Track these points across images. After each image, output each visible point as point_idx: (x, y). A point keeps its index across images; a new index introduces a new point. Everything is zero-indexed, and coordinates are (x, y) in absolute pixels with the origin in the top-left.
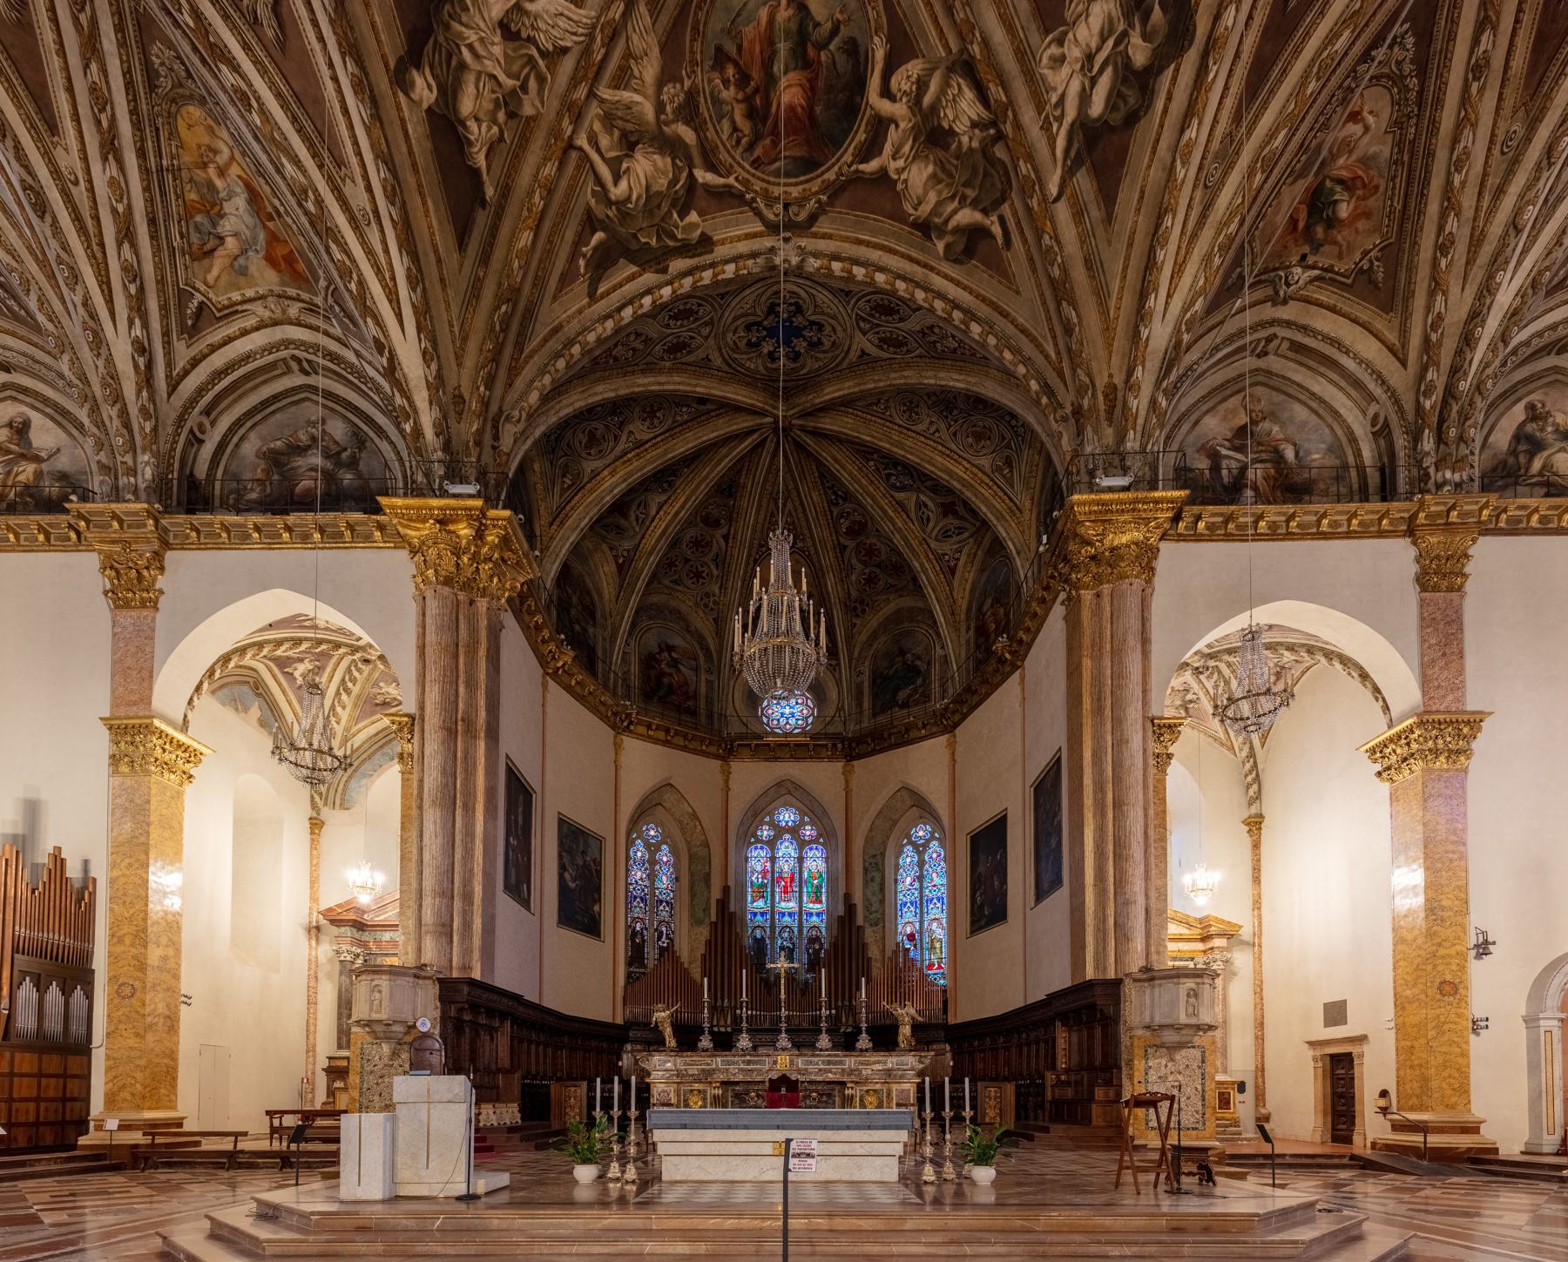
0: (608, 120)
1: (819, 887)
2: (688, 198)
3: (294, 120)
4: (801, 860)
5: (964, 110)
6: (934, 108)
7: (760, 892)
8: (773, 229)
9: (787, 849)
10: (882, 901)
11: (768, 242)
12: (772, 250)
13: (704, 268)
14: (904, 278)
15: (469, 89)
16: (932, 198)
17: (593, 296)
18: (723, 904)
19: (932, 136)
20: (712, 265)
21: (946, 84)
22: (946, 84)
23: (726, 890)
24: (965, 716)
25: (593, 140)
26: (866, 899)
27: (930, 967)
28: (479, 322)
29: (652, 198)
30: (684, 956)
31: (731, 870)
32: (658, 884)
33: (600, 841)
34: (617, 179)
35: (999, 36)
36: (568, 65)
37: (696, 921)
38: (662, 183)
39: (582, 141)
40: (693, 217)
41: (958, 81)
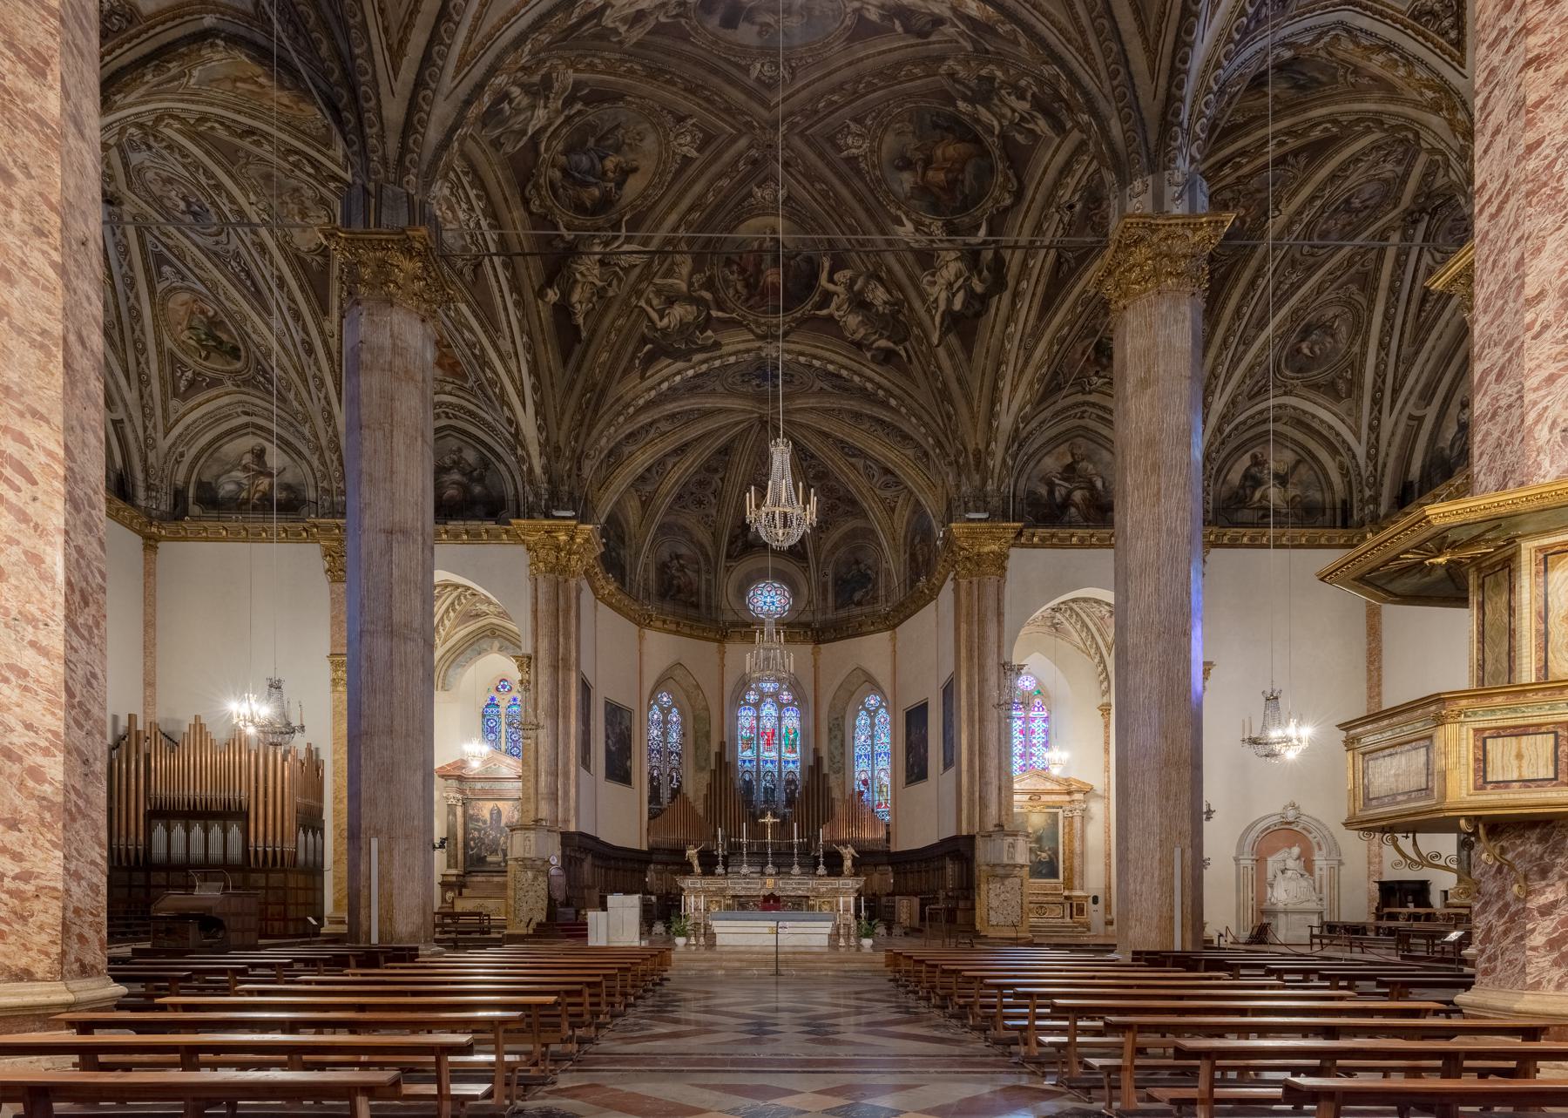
0: (658, 292)
1: (794, 740)
2: (708, 323)
3: (473, 312)
4: (780, 719)
5: (879, 295)
6: (861, 292)
7: (749, 743)
8: (762, 338)
9: (769, 710)
10: (843, 754)
11: (757, 344)
12: (760, 348)
13: (715, 359)
14: (846, 368)
15: (578, 290)
16: (862, 332)
17: (643, 378)
18: (720, 756)
19: (860, 303)
20: (721, 357)
21: (867, 283)
22: (867, 283)
23: (722, 744)
24: (902, 622)
25: (649, 302)
26: (830, 753)
27: (879, 805)
28: (572, 403)
29: (683, 325)
30: (691, 795)
31: (726, 729)
32: (670, 740)
33: (630, 712)
34: (661, 318)
35: (897, 268)
36: (637, 271)
37: (700, 768)
38: (691, 318)
39: (642, 303)
40: (709, 333)
41: (873, 283)
